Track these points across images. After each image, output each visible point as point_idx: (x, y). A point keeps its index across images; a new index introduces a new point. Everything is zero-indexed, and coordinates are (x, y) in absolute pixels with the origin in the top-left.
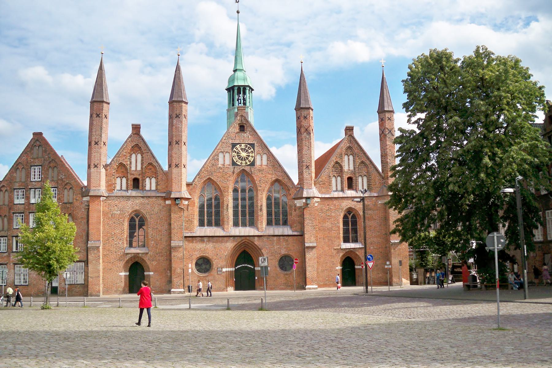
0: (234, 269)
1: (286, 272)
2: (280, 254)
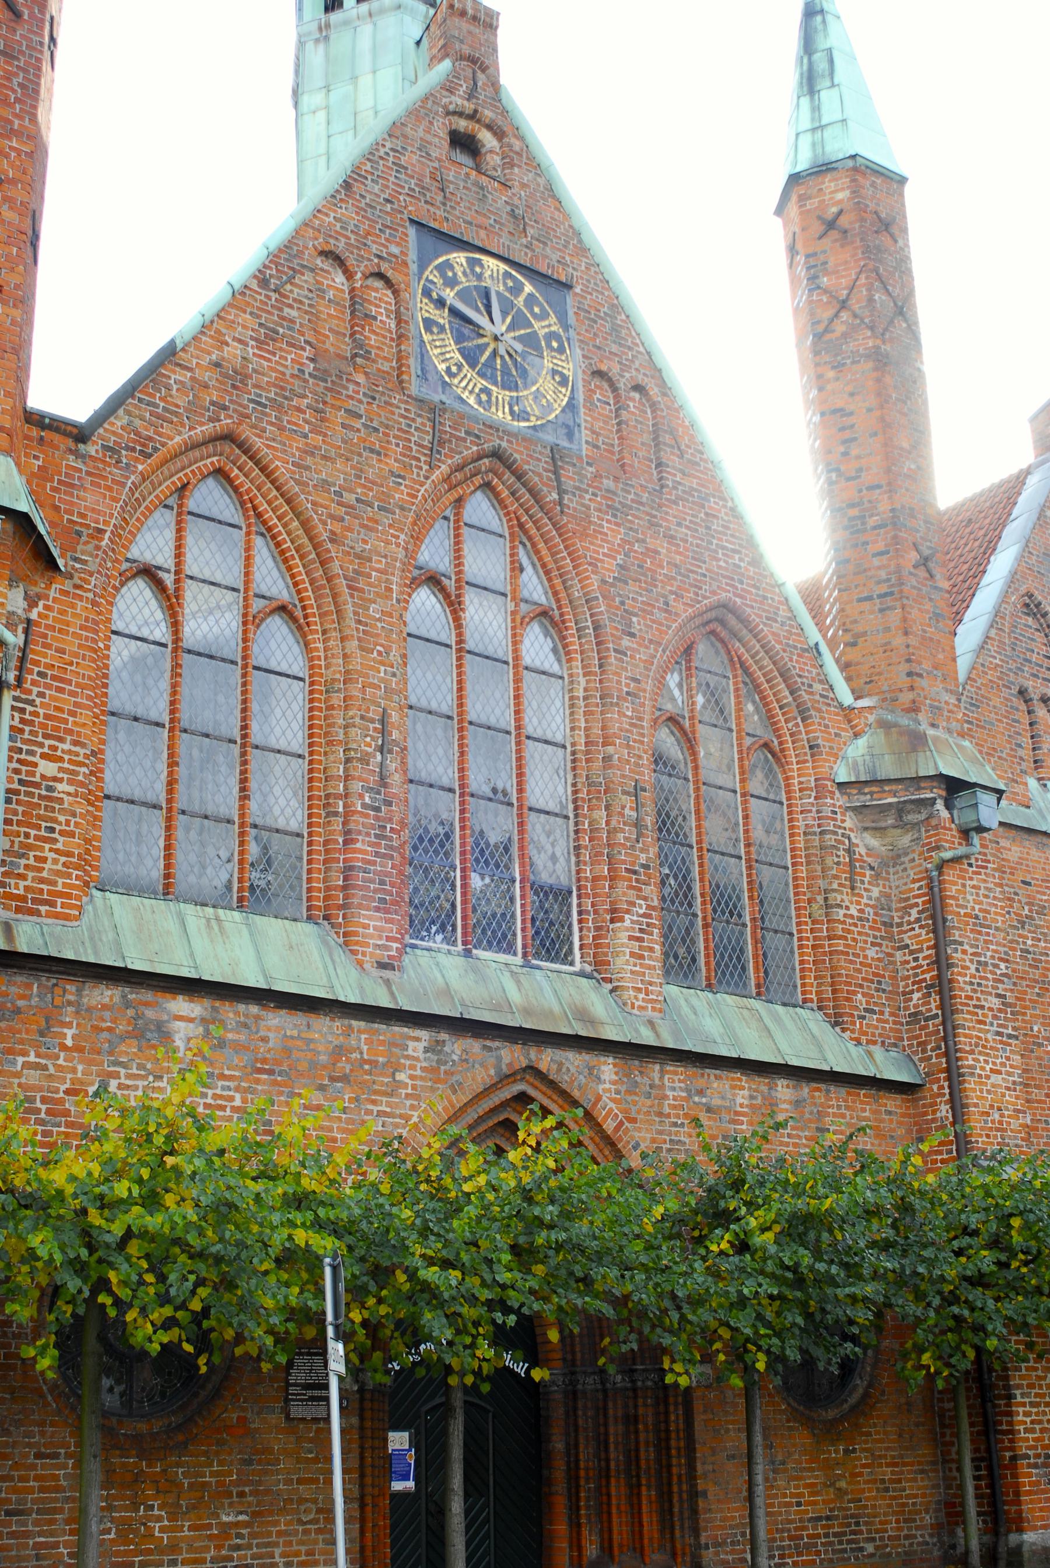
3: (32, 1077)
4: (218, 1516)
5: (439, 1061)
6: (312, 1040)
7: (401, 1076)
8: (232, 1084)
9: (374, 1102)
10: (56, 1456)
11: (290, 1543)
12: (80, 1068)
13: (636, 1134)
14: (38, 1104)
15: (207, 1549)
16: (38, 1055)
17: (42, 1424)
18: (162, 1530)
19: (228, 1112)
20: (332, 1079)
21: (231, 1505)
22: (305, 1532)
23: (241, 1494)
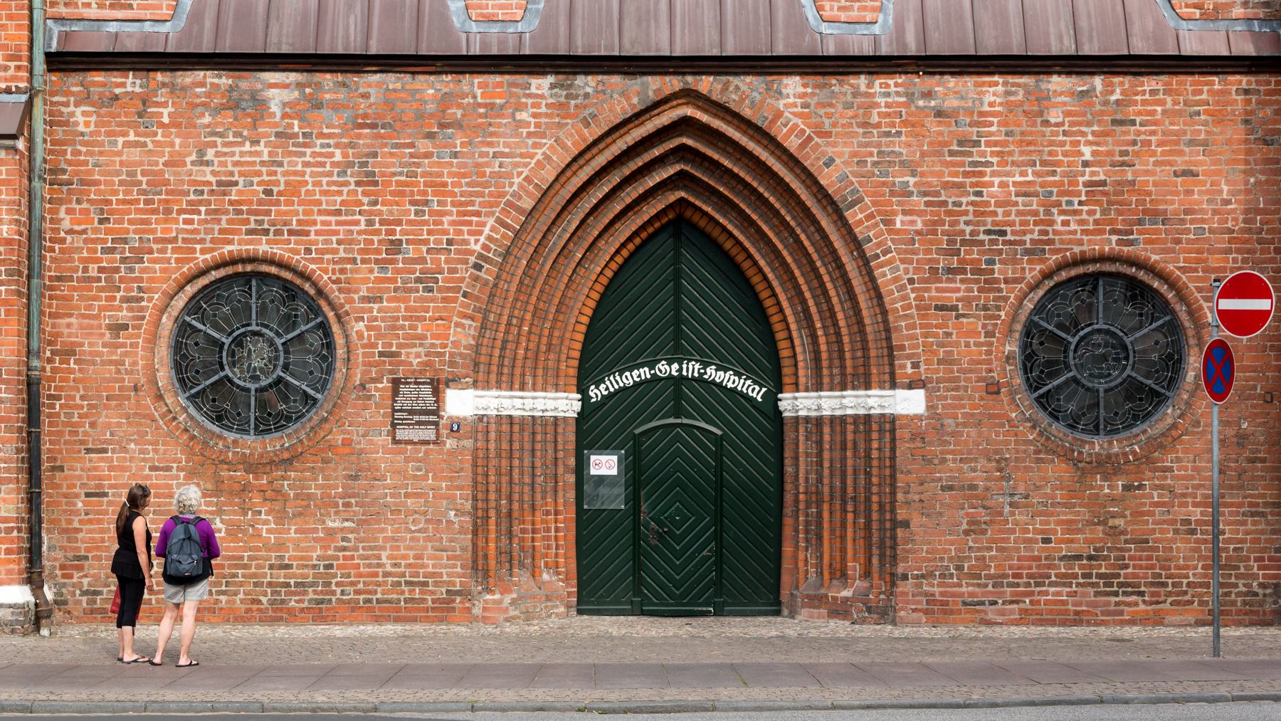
0: (566, 404)
1: (1098, 445)
2: (1034, 252)
3: (135, 154)
4: (324, 522)
5: (568, 97)
6: (417, 91)
7: (523, 116)
8: (332, 142)
9: (490, 144)
10: (169, 469)
11: (398, 548)
12: (178, 141)
13: (830, 150)
14: (139, 177)
15: (314, 549)
16: (137, 134)
17: (156, 443)
18: (269, 531)
19: (328, 168)
20: (442, 126)
21: (336, 513)
22: (412, 539)
23: (347, 505)
